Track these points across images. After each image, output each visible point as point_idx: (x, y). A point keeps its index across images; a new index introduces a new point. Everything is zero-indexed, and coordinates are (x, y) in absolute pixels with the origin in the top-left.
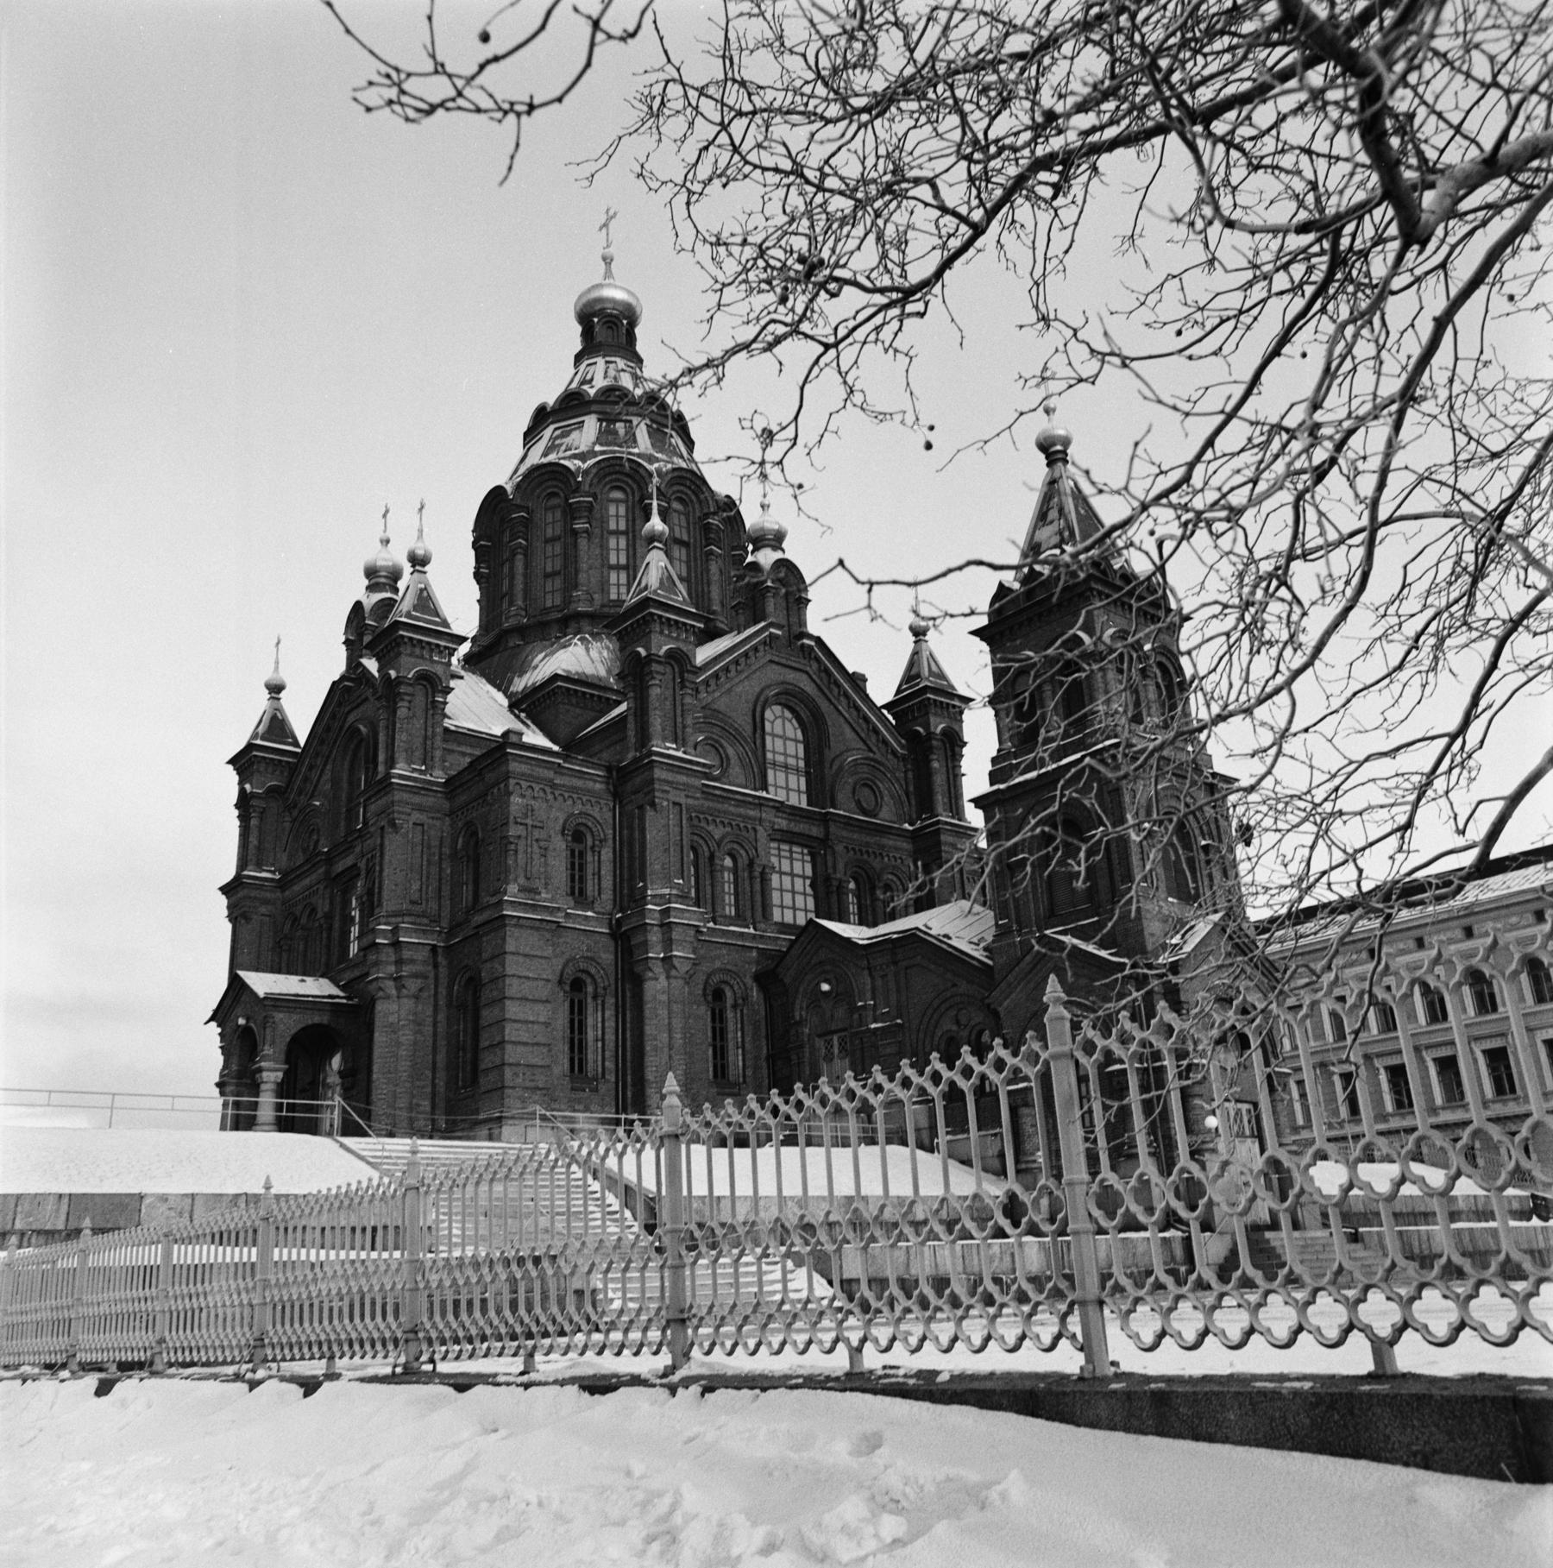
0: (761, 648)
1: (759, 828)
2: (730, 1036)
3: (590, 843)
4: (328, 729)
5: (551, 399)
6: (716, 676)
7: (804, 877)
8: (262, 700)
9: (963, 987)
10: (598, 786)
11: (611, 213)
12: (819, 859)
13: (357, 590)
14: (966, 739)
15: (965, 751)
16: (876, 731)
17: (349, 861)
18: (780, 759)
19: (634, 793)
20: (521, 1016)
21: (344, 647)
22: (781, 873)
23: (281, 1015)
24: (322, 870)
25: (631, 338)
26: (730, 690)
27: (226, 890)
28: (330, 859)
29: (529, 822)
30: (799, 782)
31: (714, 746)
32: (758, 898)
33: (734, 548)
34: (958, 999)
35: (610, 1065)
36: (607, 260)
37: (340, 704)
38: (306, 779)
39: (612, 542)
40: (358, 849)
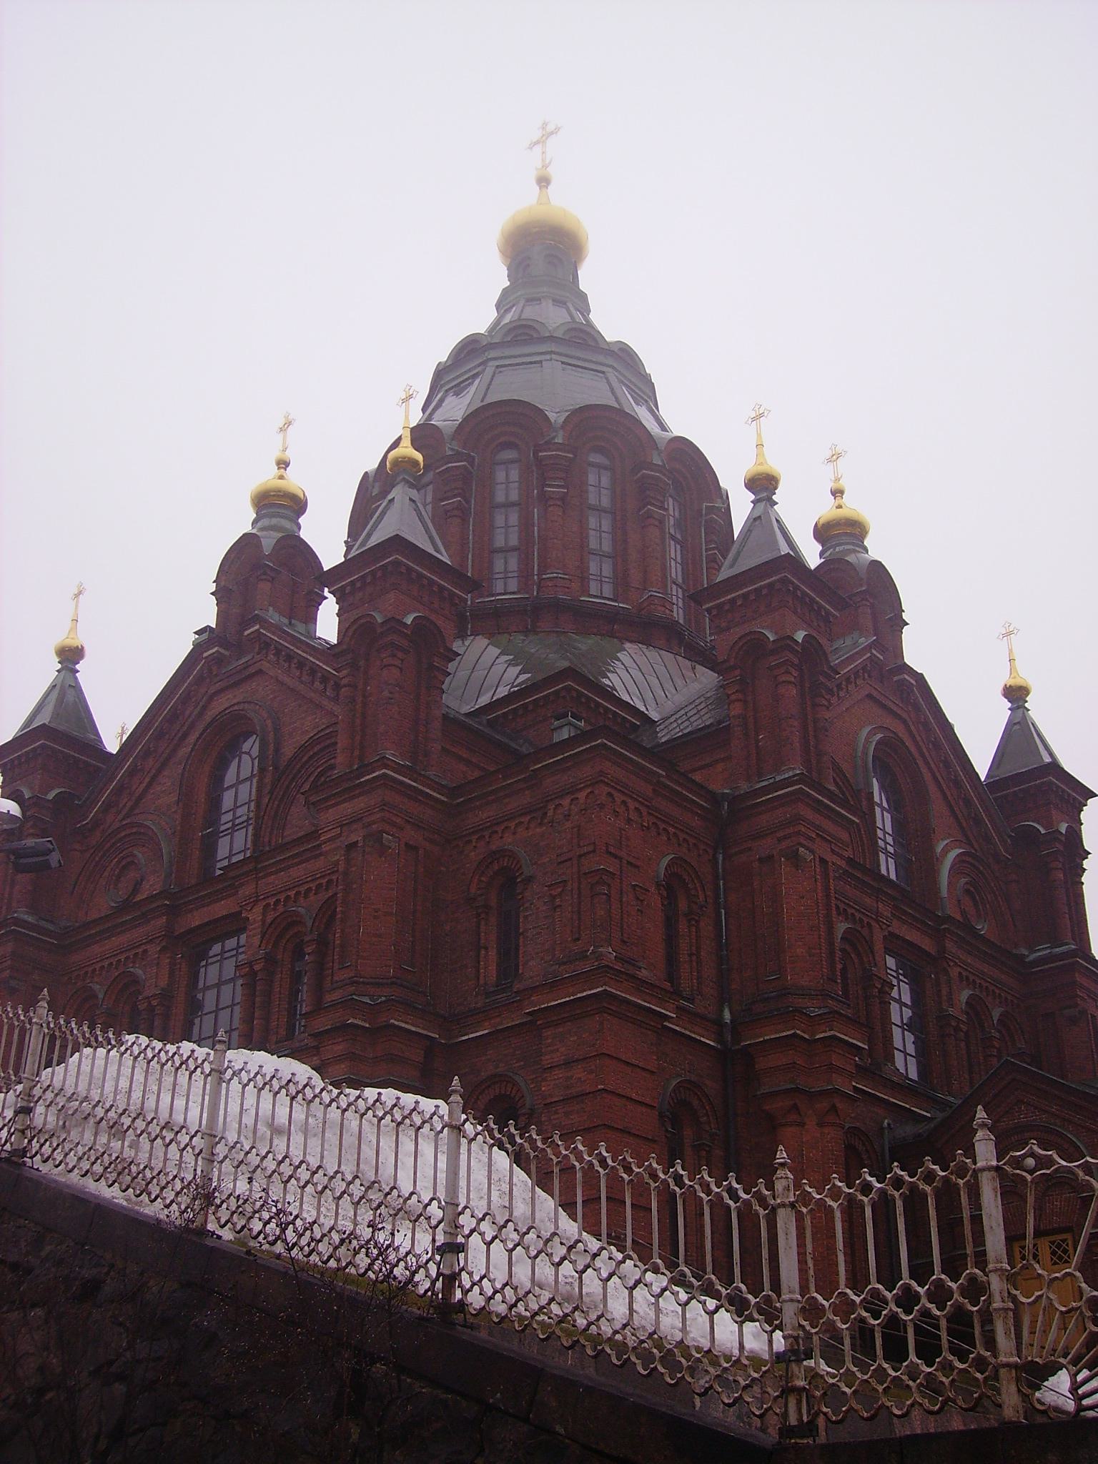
1: (873, 923)
3: (683, 905)
4: (173, 717)
8: (49, 669)
11: (551, 128)
15: (1086, 864)
17: (222, 908)
21: (213, 599)
36: (543, 181)
37: (200, 680)
39: (592, 522)
40: (246, 891)
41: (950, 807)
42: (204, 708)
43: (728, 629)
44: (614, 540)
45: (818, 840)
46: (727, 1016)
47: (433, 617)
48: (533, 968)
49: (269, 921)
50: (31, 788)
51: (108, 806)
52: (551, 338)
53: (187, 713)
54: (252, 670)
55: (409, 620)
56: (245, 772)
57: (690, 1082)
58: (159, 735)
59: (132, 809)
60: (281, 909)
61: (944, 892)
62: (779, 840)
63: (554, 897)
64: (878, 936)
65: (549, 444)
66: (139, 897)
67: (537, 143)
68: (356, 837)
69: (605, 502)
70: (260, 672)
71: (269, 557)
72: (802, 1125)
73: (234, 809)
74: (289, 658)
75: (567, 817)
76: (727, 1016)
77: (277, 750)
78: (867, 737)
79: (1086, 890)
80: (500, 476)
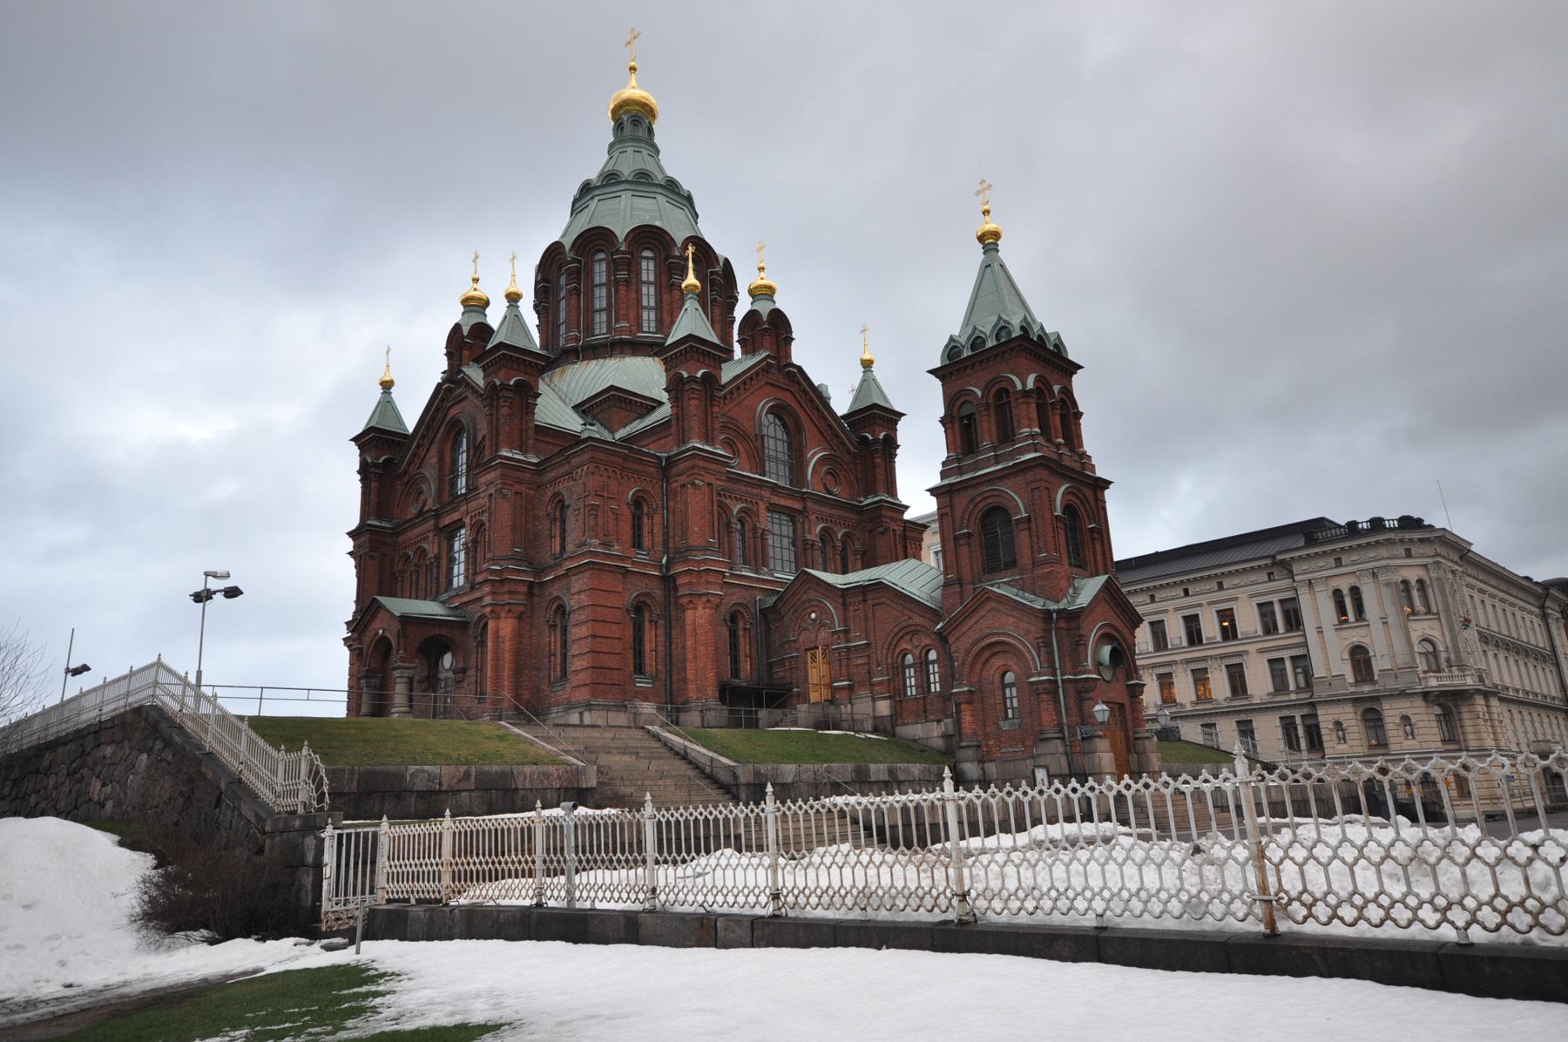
0: (761, 373)
2: (741, 648)
3: (645, 509)
4: (433, 419)
5: (593, 173)
6: (731, 392)
7: (789, 537)
9: (918, 620)
10: (652, 469)
11: (635, 32)
12: (799, 526)
13: (454, 314)
15: (898, 451)
16: (837, 436)
17: (455, 516)
18: (773, 453)
20: (603, 634)
21: (446, 358)
22: (773, 534)
24: (432, 522)
25: (650, 131)
26: (740, 403)
27: (351, 534)
28: (437, 516)
29: (605, 494)
30: (783, 470)
31: (728, 443)
32: (759, 551)
33: (728, 298)
34: (912, 628)
37: (443, 400)
38: (414, 455)
39: (644, 290)
40: (464, 508)
41: (819, 430)
42: (446, 414)
44: (656, 301)
45: (707, 475)
46: (664, 561)
48: (570, 547)
52: (626, 181)
54: (463, 396)
55: (512, 383)
58: (428, 428)
61: (809, 478)
64: (762, 506)
65: (618, 250)
66: (425, 509)
68: (492, 491)
69: (652, 278)
70: (466, 397)
71: (467, 337)
72: (695, 609)
77: (475, 438)
78: (763, 405)
80: (597, 267)
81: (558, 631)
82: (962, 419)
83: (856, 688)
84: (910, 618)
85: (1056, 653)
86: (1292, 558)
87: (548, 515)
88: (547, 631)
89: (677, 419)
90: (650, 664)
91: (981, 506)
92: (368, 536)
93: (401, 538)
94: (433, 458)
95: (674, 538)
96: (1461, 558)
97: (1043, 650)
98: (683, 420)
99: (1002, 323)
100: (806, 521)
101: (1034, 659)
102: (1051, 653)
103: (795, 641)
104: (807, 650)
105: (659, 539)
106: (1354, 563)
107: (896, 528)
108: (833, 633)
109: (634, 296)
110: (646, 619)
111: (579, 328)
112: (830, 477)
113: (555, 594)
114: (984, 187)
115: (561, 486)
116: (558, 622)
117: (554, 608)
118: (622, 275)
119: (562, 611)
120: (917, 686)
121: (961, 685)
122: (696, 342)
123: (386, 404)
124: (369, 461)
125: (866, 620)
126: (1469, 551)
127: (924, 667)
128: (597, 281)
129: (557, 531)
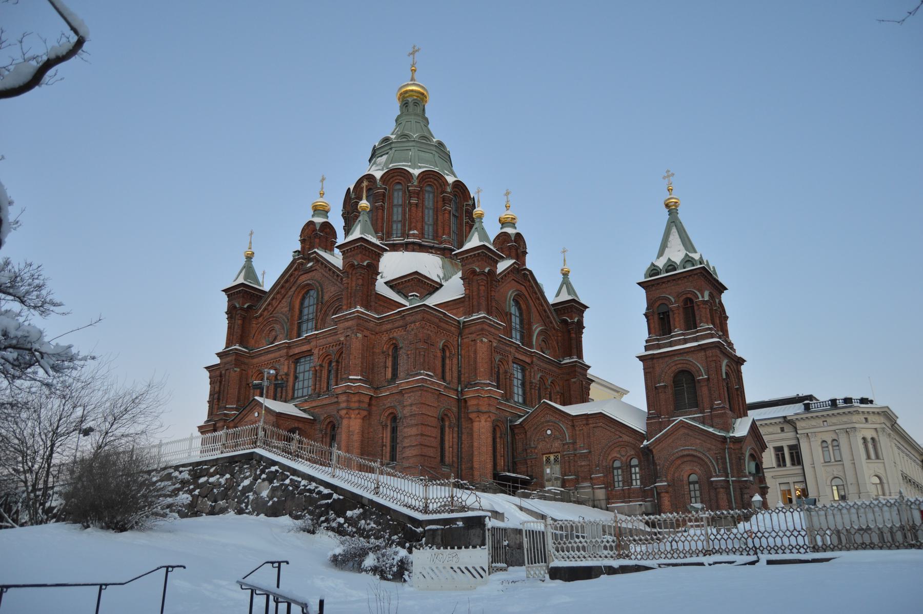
1: (509, 355)
3: (448, 354)
4: (287, 281)
9: (626, 438)
11: (416, 48)
12: (527, 373)
13: (307, 216)
14: (584, 325)
15: (584, 331)
17: (305, 348)
19: (470, 334)
21: (299, 243)
23: (282, 422)
25: (424, 110)
29: (429, 342)
35: (455, 459)
37: (296, 270)
40: (313, 344)
42: (297, 279)
43: (465, 265)
46: (460, 389)
47: (373, 262)
48: (401, 374)
49: (320, 354)
50: (239, 304)
51: (265, 309)
53: (291, 281)
54: (313, 269)
55: (365, 264)
56: (311, 303)
57: (448, 409)
58: (282, 287)
59: (273, 311)
60: (324, 350)
61: (534, 343)
62: (478, 335)
63: (408, 355)
64: (510, 359)
67: (411, 54)
70: (316, 270)
73: (308, 314)
74: (326, 266)
75: (412, 330)
76: (460, 389)
77: (322, 298)
78: (511, 294)
79: (583, 339)
80: (396, 194)
81: (389, 429)
82: (659, 314)
83: (580, 480)
84: (621, 437)
85: (728, 464)
86: (797, 419)
87: (383, 352)
88: (381, 429)
89: (469, 297)
90: (447, 460)
91: (673, 369)
92: (234, 357)
93: (256, 361)
94: (284, 307)
95: (464, 374)
96: (892, 425)
97: (720, 461)
98: (473, 299)
99: (688, 259)
100: (532, 370)
101: (714, 466)
102: (724, 463)
103: (535, 448)
104: (543, 454)
105: (455, 374)
106: (835, 424)
107: (583, 380)
108: (564, 445)
109: (421, 214)
110: (447, 426)
111: (382, 231)
112: (543, 343)
113: (389, 405)
114: (669, 175)
115: (395, 334)
116: (389, 424)
117: (386, 415)
118: (414, 201)
119: (394, 418)
120: (624, 482)
121: (661, 481)
122: (486, 250)
123: (249, 269)
124: (238, 306)
125: (589, 437)
126: (895, 423)
127: (629, 470)
128: (395, 202)
129: (389, 363)
